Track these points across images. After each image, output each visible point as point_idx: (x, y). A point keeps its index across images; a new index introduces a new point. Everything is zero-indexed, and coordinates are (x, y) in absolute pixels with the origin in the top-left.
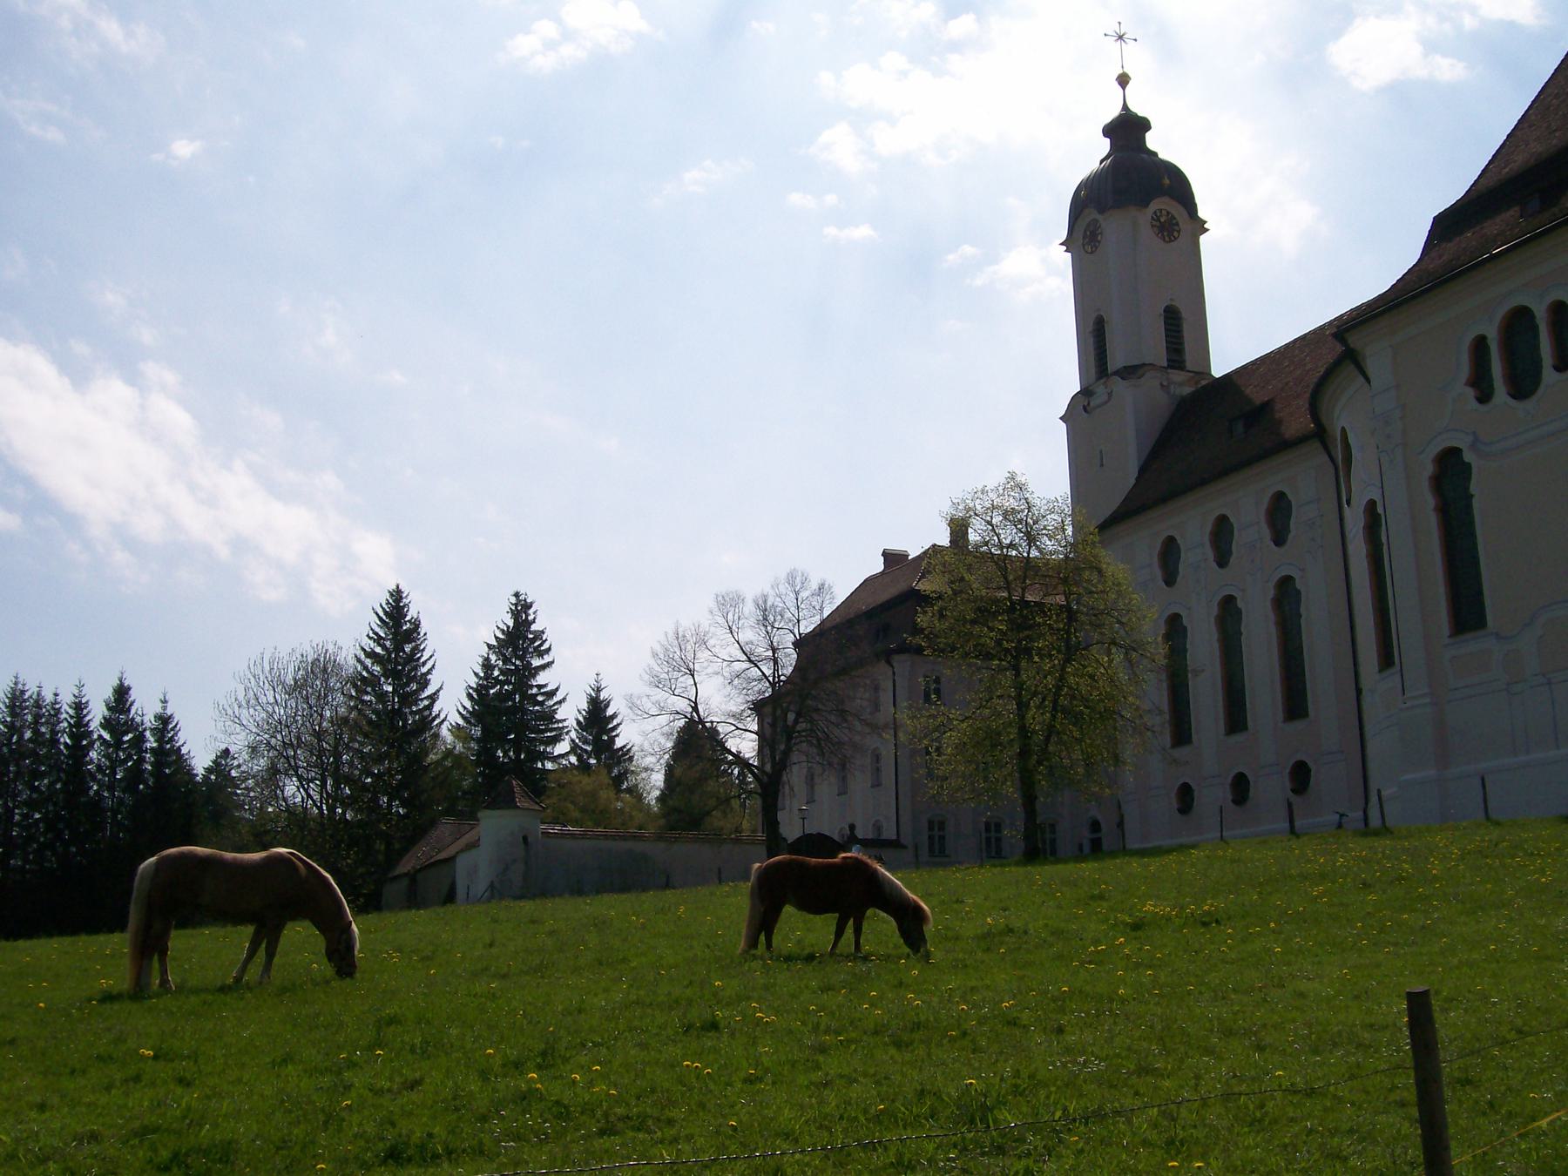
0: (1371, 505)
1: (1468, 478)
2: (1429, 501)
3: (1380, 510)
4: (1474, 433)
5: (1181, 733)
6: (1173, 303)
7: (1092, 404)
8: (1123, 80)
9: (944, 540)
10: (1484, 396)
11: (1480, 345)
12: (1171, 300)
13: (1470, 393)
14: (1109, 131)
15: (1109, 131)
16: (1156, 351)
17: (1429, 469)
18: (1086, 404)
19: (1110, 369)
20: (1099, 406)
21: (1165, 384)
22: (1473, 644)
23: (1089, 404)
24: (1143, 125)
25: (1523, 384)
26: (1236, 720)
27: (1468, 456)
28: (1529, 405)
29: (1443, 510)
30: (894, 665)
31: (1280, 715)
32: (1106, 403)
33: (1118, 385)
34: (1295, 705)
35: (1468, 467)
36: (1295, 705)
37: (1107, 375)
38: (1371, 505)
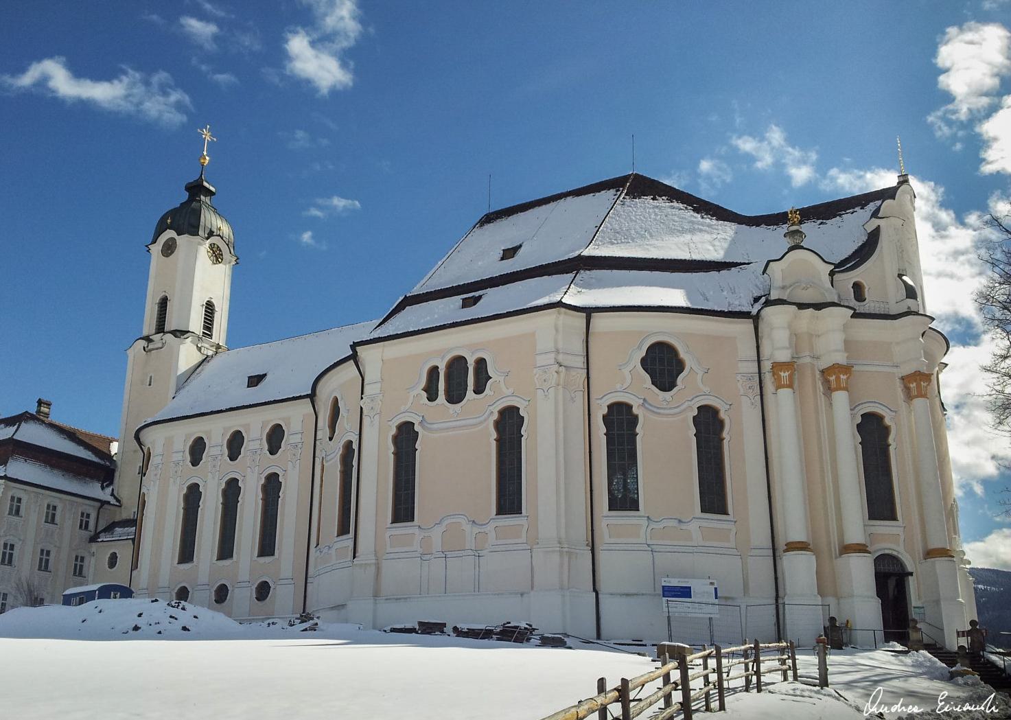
0: (349, 444)
2: (392, 448)
3: (355, 446)
4: (423, 417)
6: (212, 300)
7: (149, 348)
10: (432, 397)
11: (434, 372)
12: (211, 298)
13: (425, 395)
16: (196, 323)
17: (394, 431)
18: (146, 346)
20: (153, 349)
21: (199, 346)
22: (403, 529)
23: (148, 347)
25: (455, 396)
27: (417, 428)
29: (397, 454)
34: (267, 546)
36: (267, 546)
37: (163, 332)
38: (349, 444)
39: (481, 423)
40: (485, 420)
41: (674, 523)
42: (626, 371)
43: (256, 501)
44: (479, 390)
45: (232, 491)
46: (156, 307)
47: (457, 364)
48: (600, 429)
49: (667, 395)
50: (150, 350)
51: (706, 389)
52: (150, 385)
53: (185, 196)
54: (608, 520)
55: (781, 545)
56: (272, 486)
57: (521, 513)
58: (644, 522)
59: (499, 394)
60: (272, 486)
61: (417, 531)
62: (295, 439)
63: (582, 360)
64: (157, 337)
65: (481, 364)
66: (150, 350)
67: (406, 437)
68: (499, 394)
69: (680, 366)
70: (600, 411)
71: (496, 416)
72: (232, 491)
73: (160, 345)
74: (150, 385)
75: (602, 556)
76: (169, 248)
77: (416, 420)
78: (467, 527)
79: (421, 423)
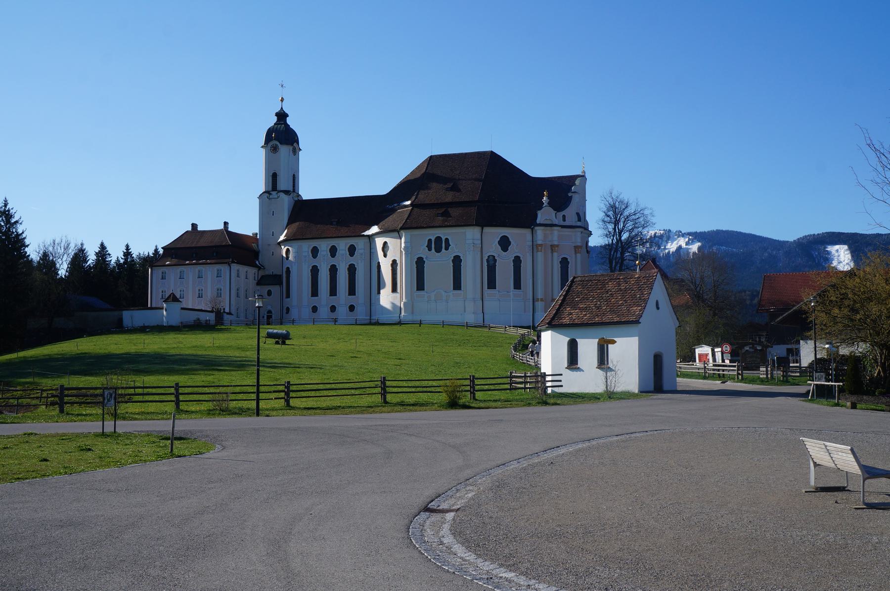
1: (424, 263)
3: (398, 262)
5: (315, 292)
7: (271, 197)
8: (282, 100)
9: (221, 227)
10: (430, 249)
11: (430, 241)
13: (427, 248)
14: (277, 114)
15: (277, 114)
17: (416, 260)
19: (278, 188)
22: (421, 293)
24: (287, 115)
25: (438, 250)
26: (333, 291)
28: (439, 254)
30: (232, 266)
31: (347, 294)
32: (278, 198)
33: (282, 195)
34: (352, 291)
35: (425, 261)
36: (352, 291)
39: (447, 260)
40: (449, 259)
41: (506, 293)
42: (494, 245)
43: (346, 275)
44: (447, 249)
45: (333, 270)
46: (271, 178)
47: (438, 239)
48: (485, 264)
49: (505, 253)
50: (271, 199)
51: (517, 251)
52: (273, 215)
53: (275, 119)
54: (487, 292)
55: (535, 299)
56: (352, 270)
57: (461, 289)
58: (497, 292)
59: (454, 251)
60: (352, 270)
61: (425, 293)
62: (361, 251)
63: (480, 241)
64: (274, 193)
65: (447, 240)
66: (271, 199)
67: (420, 263)
68: (454, 251)
69: (509, 243)
70: (485, 258)
71: (452, 258)
72: (333, 270)
73: (277, 197)
74: (273, 215)
75: (485, 303)
76: (275, 149)
77: (424, 257)
78: (444, 293)
79: (426, 258)
